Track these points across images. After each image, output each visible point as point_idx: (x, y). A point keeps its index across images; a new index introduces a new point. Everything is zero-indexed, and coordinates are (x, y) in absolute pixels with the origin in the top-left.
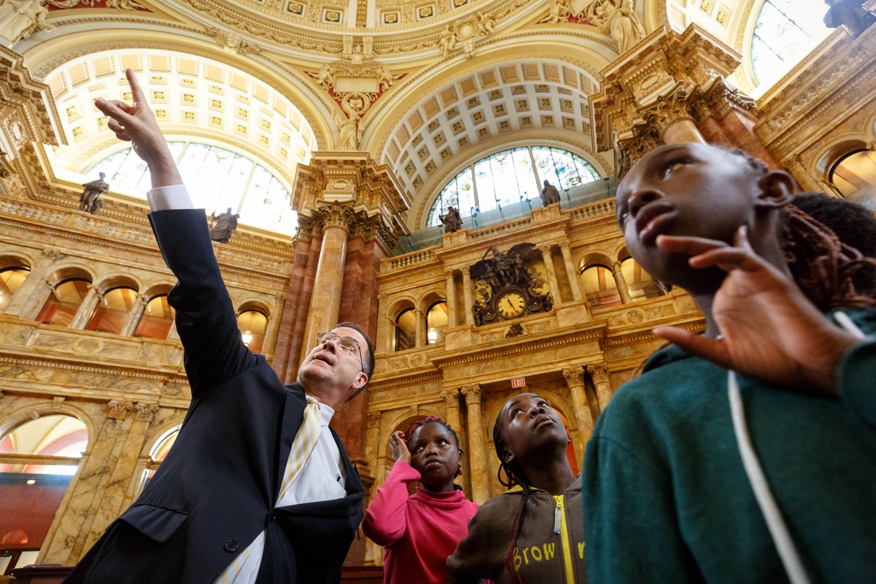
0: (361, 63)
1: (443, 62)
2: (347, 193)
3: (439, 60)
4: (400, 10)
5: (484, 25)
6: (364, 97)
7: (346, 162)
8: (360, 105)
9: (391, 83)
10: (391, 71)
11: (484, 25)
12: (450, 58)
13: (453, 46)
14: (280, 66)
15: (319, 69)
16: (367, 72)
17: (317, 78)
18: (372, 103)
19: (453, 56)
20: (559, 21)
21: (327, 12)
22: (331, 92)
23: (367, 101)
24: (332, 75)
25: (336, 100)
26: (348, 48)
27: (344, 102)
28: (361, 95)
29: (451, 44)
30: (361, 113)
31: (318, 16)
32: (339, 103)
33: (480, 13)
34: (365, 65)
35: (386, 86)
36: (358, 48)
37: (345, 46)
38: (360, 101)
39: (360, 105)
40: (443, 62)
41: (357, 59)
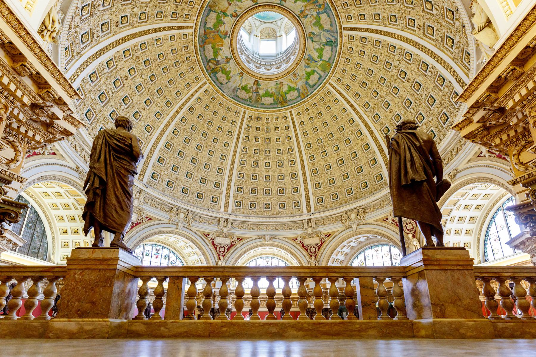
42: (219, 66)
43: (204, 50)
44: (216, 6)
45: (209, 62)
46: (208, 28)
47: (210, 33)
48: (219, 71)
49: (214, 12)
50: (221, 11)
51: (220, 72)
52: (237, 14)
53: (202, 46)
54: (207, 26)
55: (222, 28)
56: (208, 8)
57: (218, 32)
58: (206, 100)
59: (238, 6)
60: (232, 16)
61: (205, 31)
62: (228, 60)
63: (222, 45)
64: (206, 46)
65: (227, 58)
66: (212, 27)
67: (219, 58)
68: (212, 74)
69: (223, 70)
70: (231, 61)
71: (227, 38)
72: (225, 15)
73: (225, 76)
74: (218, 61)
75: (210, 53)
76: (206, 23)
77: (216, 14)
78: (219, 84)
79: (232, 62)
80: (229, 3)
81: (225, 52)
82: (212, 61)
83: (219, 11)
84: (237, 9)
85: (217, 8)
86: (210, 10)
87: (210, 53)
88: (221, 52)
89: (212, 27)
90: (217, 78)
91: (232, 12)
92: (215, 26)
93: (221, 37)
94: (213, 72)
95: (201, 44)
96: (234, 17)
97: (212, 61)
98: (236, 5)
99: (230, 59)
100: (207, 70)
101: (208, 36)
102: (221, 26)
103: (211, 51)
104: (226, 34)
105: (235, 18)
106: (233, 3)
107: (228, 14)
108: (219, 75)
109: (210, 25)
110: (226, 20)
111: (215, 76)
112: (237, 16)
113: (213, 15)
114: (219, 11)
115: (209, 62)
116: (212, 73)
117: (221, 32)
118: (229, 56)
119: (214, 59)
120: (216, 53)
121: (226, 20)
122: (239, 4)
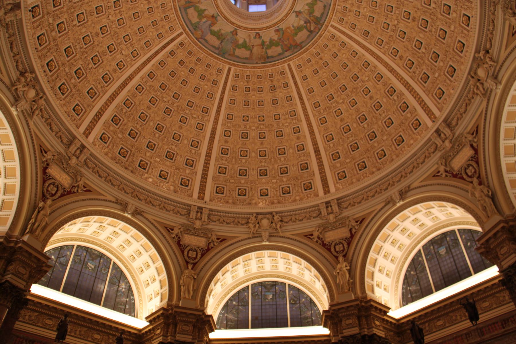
0: (200, 227)
1: (248, 238)
2: (190, 335)
3: (246, 236)
4: (226, 186)
5: (276, 225)
6: (198, 251)
7: (191, 314)
8: (194, 256)
9: (216, 244)
10: (216, 235)
11: (276, 225)
12: (253, 237)
13: (257, 231)
14: (152, 224)
15: (174, 227)
16: (202, 233)
17: (172, 233)
18: (203, 255)
19: (255, 237)
20: (317, 242)
21: (182, 179)
22: (179, 243)
23: (199, 255)
24: (181, 232)
25: (181, 249)
26: (193, 215)
27: (186, 253)
28: (197, 249)
29: (256, 229)
30: (195, 262)
31: (177, 182)
32: (183, 252)
33: (274, 214)
34: (200, 229)
35: (212, 245)
36: (199, 214)
37: (192, 212)
38: (195, 253)
39: (194, 256)
40: (248, 238)
41: (198, 224)
42: (309, 19)
43: (302, 42)
44: (261, 55)
45: (311, 32)
46: (282, 49)
47: (286, 45)
48: (314, 16)
49: (267, 53)
50: (263, 48)
51: (314, 14)
52: (256, 35)
53: (299, 46)
54: (281, 51)
55: (276, 38)
56: (267, 60)
57: (280, 39)
58: (350, 18)
59: (250, 39)
60: (260, 37)
61: (287, 51)
62: (298, 13)
63: (289, 28)
64: (298, 43)
65: (297, 16)
66: (280, 47)
67: (302, 23)
68: (321, 22)
69: (311, 13)
70: (297, 9)
71: (280, 27)
72: (263, 43)
73: (315, 7)
74: (305, 23)
75: (302, 35)
76: (280, 54)
77: (268, 51)
78: (327, 8)
79: (298, 8)
80: (253, 48)
81: (293, 21)
82: (308, 28)
83: (264, 50)
84: (252, 38)
85: (263, 54)
86: (268, 57)
87: (302, 35)
88: (295, 25)
89: (280, 47)
90: (322, 14)
91: (257, 40)
92: (277, 45)
93: (283, 33)
94: (319, 22)
95: (299, 48)
96: (259, 35)
97: (308, 28)
98: (250, 42)
99: (296, 12)
100: (320, 30)
101: (289, 46)
102: (274, 40)
103: (300, 34)
104: (277, 31)
105: (261, 34)
106: (251, 45)
107: (261, 41)
108: (317, 14)
109: (279, 50)
110: (267, 40)
111: (321, 18)
112: (258, 33)
113: (271, 52)
114: (264, 50)
115: (311, 32)
116: (319, 22)
117: (279, 36)
118: (294, 15)
119: (306, 27)
120: (299, 29)
121: (267, 40)
122: (247, 40)
